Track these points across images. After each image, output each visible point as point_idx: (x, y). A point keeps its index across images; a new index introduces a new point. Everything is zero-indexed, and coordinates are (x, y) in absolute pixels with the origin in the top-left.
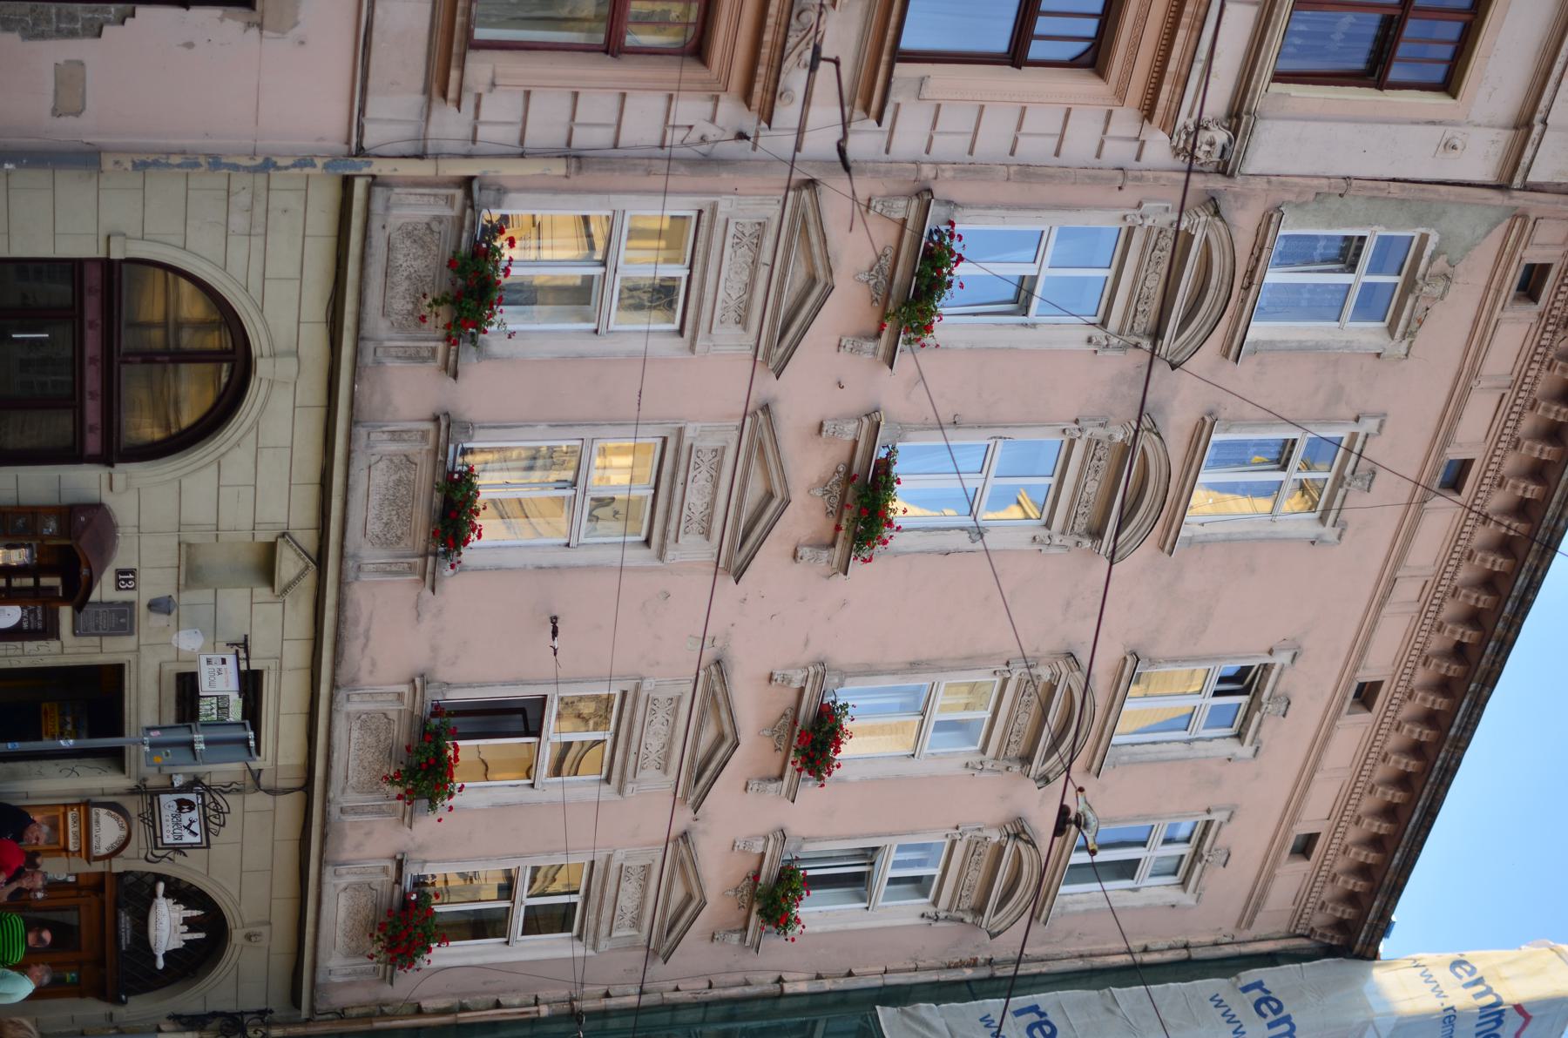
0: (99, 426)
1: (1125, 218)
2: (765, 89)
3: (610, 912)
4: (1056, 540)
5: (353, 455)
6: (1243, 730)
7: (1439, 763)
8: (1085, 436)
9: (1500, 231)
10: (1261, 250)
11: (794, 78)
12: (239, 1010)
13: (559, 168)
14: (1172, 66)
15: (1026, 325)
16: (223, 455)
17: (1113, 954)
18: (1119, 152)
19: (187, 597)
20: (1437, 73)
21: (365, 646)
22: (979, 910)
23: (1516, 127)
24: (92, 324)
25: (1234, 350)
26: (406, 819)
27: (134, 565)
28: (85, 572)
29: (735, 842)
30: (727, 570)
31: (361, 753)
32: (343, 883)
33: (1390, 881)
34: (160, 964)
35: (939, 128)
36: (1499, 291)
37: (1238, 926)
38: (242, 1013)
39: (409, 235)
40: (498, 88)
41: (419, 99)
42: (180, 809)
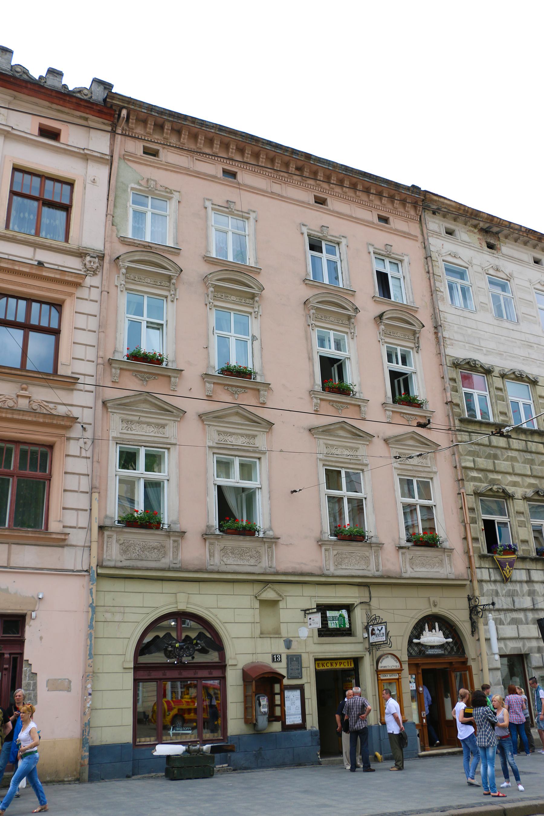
1: (122, 291)
3: (420, 467)
4: (256, 310)
5: (220, 571)
6: (336, 242)
7: (344, 172)
8: (212, 301)
10: (135, 243)
11: (62, 410)
12: (468, 608)
13: (95, 496)
14: (58, 276)
15: (167, 324)
16: (220, 621)
17: (431, 284)
18: (95, 294)
19: (284, 634)
20: (67, 188)
21: (305, 564)
22: (414, 333)
23: (87, 160)
25: (176, 251)
26: (380, 546)
27: (270, 656)
30: (270, 429)
32: (409, 570)
33: (393, 187)
34: (450, 640)
35: (83, 358)
37: (417, 241)
38: (470, 607)
40: (61, 519)
41: (66, 549)
42: (374, 634)
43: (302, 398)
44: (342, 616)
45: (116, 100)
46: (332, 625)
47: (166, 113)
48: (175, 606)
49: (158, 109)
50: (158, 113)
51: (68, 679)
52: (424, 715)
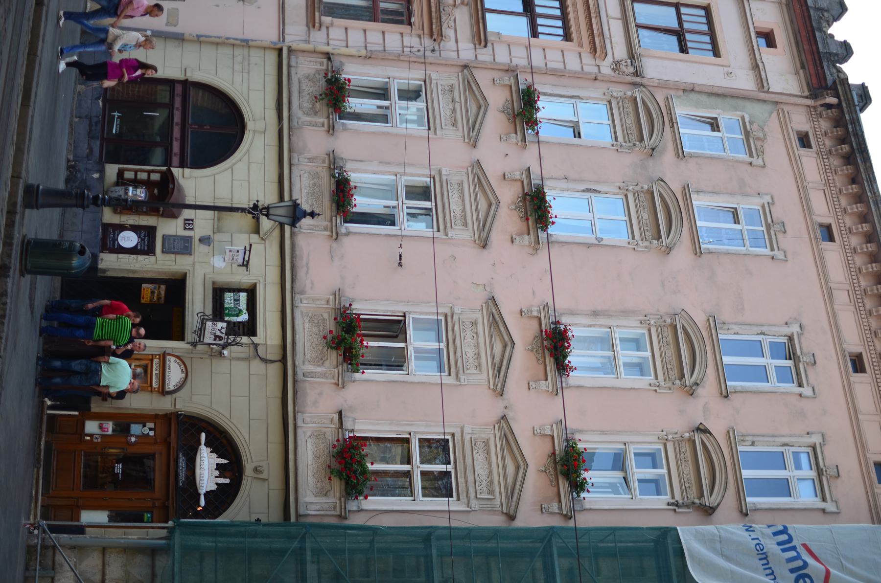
0: (179, 153)
1: (604, 94)
2: (437, 26)
5: (292, 168)
9: (775, 115)
10: (670, 110)
11: (449, 33)
14: (595, 31)
16: (234, 164)
18: (590, 68)
19: (218, 237)
21: (307, 273)
24: (177, 109)
28: (171, 186)
29: (534, 427)
31: (311, 338)
36: (790, 139)
39: (307, 77)
41: (305, 28)
43: (534, 293)
44: (239, 313)
45: (842, 88)
46: (228, 297)
47: (859, 139)
48: (251, 119)
49: (858, 128)
50: (853, 131)
51: (178, 24)
52: (96, 438)
